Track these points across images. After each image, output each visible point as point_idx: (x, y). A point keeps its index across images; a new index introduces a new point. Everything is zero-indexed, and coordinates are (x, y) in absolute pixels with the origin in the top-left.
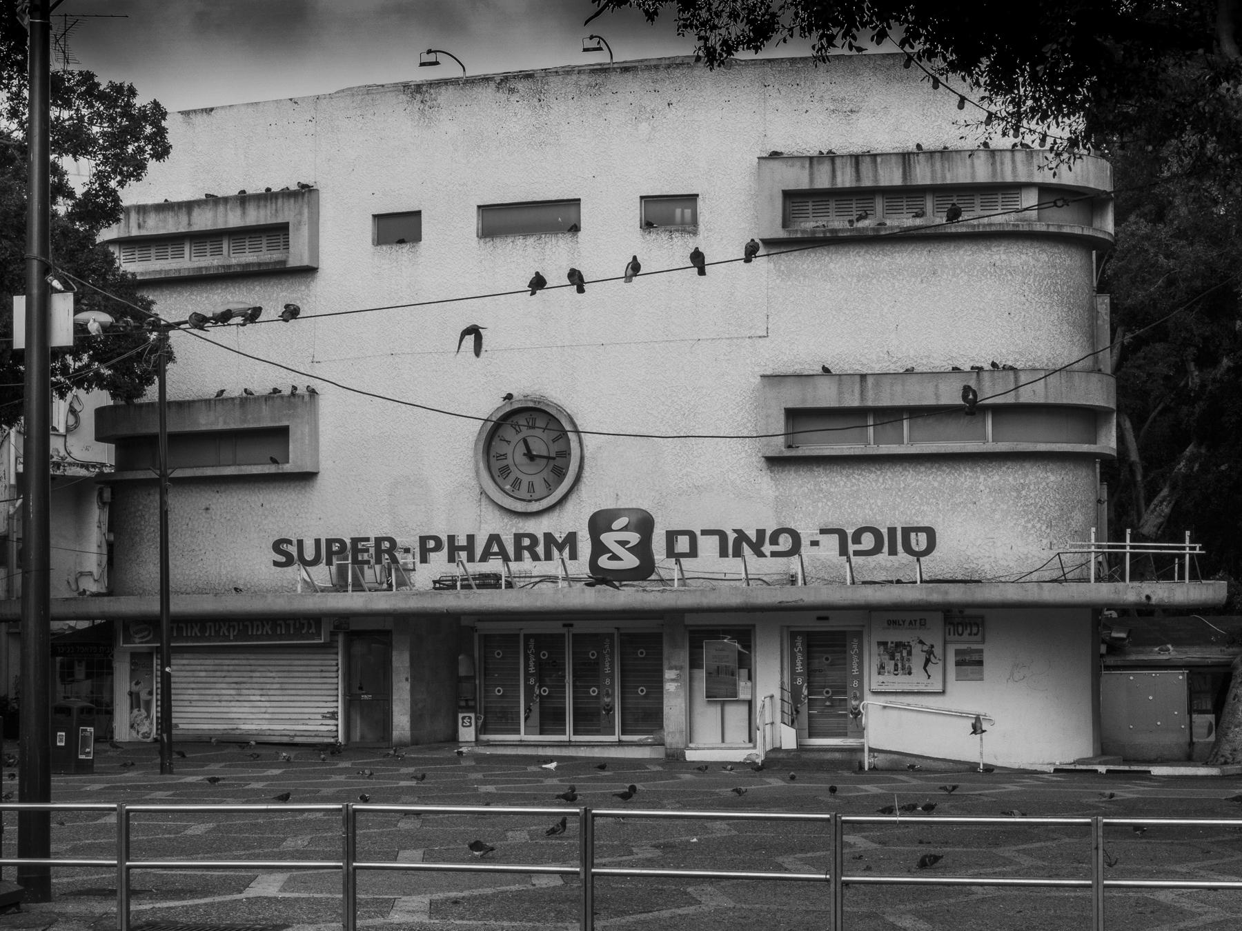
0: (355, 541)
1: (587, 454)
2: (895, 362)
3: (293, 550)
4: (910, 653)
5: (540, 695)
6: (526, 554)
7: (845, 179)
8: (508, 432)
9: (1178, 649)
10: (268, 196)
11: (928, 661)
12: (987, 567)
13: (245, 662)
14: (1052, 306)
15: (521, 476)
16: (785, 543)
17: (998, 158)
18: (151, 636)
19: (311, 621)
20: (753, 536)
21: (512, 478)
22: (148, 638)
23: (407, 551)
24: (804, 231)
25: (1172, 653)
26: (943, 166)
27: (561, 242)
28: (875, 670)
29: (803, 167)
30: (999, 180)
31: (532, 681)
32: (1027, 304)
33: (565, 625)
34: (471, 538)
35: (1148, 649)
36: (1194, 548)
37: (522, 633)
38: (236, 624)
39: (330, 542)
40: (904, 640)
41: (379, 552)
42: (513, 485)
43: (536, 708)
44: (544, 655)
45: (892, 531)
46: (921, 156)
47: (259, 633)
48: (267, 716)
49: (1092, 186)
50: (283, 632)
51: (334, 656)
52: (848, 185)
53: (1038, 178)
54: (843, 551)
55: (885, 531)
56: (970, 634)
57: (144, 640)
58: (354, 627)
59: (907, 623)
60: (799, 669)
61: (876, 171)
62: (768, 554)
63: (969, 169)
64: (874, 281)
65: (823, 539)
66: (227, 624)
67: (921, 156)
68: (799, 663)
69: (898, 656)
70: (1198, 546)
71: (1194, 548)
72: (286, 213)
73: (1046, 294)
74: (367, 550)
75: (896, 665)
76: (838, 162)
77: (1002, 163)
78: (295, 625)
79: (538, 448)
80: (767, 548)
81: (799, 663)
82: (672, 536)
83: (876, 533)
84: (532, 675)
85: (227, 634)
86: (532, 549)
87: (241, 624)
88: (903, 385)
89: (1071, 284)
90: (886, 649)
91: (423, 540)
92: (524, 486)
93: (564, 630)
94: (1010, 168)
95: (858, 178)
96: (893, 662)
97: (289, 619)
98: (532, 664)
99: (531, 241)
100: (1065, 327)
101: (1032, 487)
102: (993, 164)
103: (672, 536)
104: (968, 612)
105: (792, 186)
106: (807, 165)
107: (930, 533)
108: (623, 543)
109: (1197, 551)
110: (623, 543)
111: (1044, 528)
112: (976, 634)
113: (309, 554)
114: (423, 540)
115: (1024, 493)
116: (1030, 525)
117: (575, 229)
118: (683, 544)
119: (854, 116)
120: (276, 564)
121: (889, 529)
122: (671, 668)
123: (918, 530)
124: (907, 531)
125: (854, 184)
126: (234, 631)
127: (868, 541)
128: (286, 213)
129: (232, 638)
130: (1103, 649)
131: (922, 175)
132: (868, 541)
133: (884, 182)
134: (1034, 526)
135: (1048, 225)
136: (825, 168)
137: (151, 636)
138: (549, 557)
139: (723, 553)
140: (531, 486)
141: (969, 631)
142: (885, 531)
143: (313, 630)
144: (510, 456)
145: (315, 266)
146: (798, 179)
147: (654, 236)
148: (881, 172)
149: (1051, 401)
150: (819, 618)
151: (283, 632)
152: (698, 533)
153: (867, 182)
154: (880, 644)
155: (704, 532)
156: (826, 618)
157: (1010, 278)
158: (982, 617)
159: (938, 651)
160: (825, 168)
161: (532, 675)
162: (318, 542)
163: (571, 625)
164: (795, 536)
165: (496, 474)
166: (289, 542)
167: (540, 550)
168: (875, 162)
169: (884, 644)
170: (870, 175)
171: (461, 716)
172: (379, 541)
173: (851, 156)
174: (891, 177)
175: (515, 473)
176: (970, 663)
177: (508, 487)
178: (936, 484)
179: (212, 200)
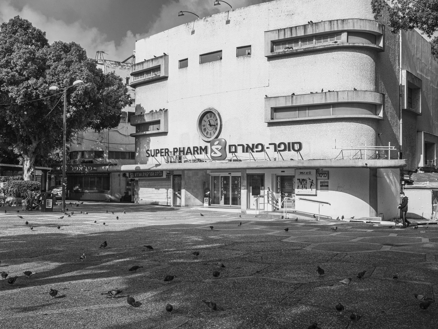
0: (161, 149)
1: (223, 123)
2: (304, 91)
4: (306, 183)
5: (224, 193)
6: (196, 153)
7: (288, 36)
8: (205, 118)
9: (431, 183)
10: (156, 58)
11: (311, 185)
12: (330, 155)
13: (145, 183)
14: (353, 70)
15: (209, 131)
16: (260, 148)
17: (332, 23)
20: (251, 146)
21: (206, 132)
23: (171, 152)
24: (276, 53)
25: (428, 184)
26: (316, 28)
27: (218, 63)
28: (296, 187)
29: (276, 33)
30: (333, 30)
31: (222, 189)
32: (344, 70)
33: (229, 174)
34: (184, 148)
35: (420, 183)
36: (392, 148)
37: (220, 176)
39: (156, 150)
40: (305, 178)
42: (207, 134)
43: (223, 197)
44: (225, 182)
45: (289, 143)
46: (309, 25)
48: (158, 198)
49: (368, 30)
51: (170, 182)
52: (289, 37)
53: (346, 28)
54: (275, 150)
55: (287, 144)
56: (324, 177)
58: (175, 174)
59: (305, 173)
60: (279, 187)
61: (297, 32)
62: (255, 151)
63: (323, 28)
64: (298, 67)
65: (270, 146)
67: (309, 25)
68: (279, 185)
69: (303, 183)
70: (393, 147)
71: (392, 148)
72: (161, 62)
73: (351, 66)
75: (302, 186)
76: (286, 30)
77: (334, 25)
79: (212, 123)
80: (255, 150)
81: (279, 185)
82: (230, 146)
83: (284, 144)
84: (222, 188)
86: (197, 151)
88: (304, 98)
89: (362, 62)
90: (299, 181)
91: (174, 149)
92: (209, 134)
93: (229, 175)
94: (336, 26)
95: (292, 34)
96: (301, 185)
98: (222, 185)
99: (211, 63)
100: (359, 77)
101: (345, 129)
102: (331, 25)
103: (230, 146)
104: (324, 169)
105: (273, 39)
106: (277, 32)
107: (300, 144)
108: (217, 149)
109: (393, 149)
110: (217, 149)
111: (349, 142)
112: (326, 177)
114: (174, 149)
115: (342, 131)
116: (344, 142)
117: (221, 58)
118: (233, 149)
119: (293, 16)
121: (288, 143)
122: (243, 186)
123: (297, 143)
124: (293, 144)
125: (290, 37)
127: (282, 147)
128: (161, 62)
130: (403, 183)
131: (310, 31)
132: (282, 147)
133: (299, 35)
134: (345, 142)
135: (349, 43)
136: (282, 32)
138: (201, 153)
139: (243, 152)
140: (211, 133)
141: (323, 176)
142: (287, 144)
144: (206, 125)
145: (167, 76)
146: (275, 37)
147: (240, 59)
148: (298, 32)
149: (350, 101)
150: (282, 172)
152: (237, 145)
153: (294, 36)
154: (298, 179)
155: (239, 145)
156: (284, 172)
157: (338, 62)
158: (328, 172)
159: (314, 182)
160: (282, 32)
161: (222, 188)
162: (154, 150)
163: (230, 174)
164: (262, 145)
165: (203, 130)
167: (199, 152)
168: (296, 29)
169: (299, 179)
170: (295, 33)
171: (205, 198)
172: (165, 149)
173: (289, 28)
174: (301, 33)
175: (207, 130)
176: (325, 186)
177: (205, 134)
178: (315, 129)
179: (146, 61)
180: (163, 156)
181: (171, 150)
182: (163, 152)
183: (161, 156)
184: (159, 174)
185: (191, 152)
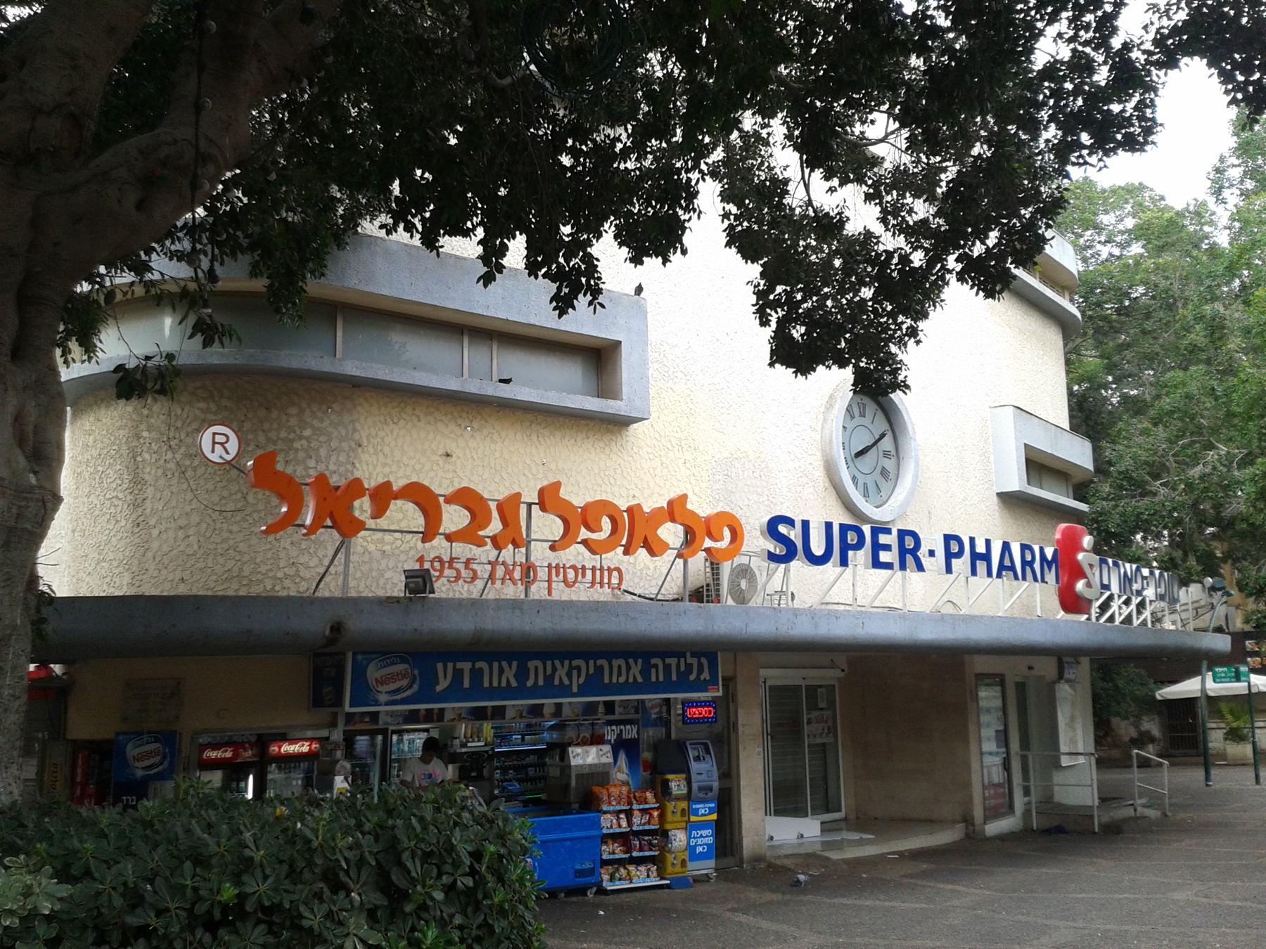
18: (416, 687)
22: (409, 693)
34: (988, 542)
38: (581, 663)
41: (903, 551)
47: (622, 680)
50: (661, 679)
57: (399, 697)
66: (567, 663)
74: (887, 548)
78: (678, 665)
85: (566, 682)
87: (591, 662)
97: (671, 655)
113: (818, 549)
126: (579, 676)
129: (575, 689)
137: (416, 687)
143: (706, 675)
151: (661, 679)
172: (902, 534)
180: (888, 566)
181: (932, 540)
182: (887, 548)
184: (684, 675)
185: (1012, 568)
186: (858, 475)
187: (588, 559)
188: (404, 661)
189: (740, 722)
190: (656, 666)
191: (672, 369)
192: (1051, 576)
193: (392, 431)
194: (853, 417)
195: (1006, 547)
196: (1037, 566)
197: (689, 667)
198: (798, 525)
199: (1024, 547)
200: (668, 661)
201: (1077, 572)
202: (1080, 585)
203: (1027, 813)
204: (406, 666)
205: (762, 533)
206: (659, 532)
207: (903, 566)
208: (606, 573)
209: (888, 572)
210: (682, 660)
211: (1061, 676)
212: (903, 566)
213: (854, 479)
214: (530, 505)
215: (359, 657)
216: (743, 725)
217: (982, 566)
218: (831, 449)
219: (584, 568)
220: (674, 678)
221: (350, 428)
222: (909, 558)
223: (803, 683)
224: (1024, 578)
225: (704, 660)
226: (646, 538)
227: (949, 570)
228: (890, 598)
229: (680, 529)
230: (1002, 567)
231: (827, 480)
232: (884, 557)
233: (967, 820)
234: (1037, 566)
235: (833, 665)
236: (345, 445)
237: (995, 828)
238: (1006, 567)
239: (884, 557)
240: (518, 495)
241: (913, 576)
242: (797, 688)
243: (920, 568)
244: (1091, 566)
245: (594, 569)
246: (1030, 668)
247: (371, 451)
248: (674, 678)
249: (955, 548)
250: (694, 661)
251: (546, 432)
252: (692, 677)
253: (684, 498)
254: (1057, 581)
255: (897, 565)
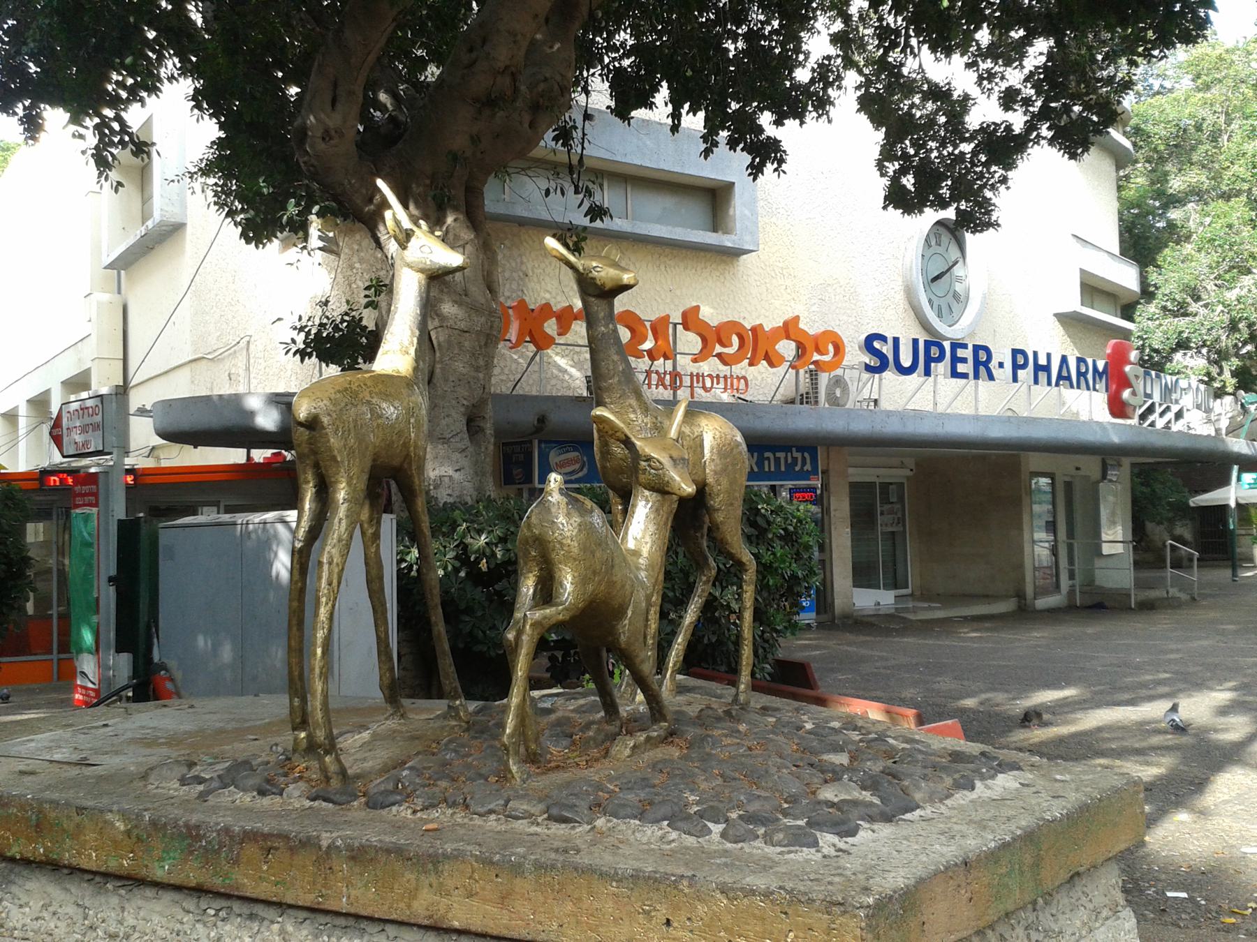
3: (887, 349)
18: (585, 470)
19: (806, 455)
22: (580, 474)
34: (1049, 356)
41: (977, 363)
50: (772, 469)
57: (573, 478)
74: (964, 360)
91: (1015, 352)
113: (906, 362)
114: (1015, 352)
120: (868, 368)
137: (585, 470)
143: (808, 467)
151: (772, 469)
162: (915, 342)
166: (883, 338)
172: (977, 348)
181: (1001, 354)
182: (964, 360)
183: (955, 374)
185: (1069, 378)
186: (933, 298)
187: (724, 370)
188: (575, 449)
189: (832, 508)
190: (768, 459)
191: (775, 206)
192: (1101, 385)
193: (550, 264)
194: (930, 246)
195: (1064, 359)
196: (1090, 376)
197: (795, 460)
198: (890, 342)
199: (1080, 360)
200: (778, 455)
201: (1124, 382)
202: (1126, 394)
203: (1071, 592)
204: (577, 454)
205: (860, 348)
206: (777, 347)
207: (976, 376)
208: (735, 381)
209: (963, 381)
210: (789, 454)
211: (1104, 477)
212: (976, 376)
213: (930, 301)
214: (675, 325)
215: (543, 446)
216: (835, 510)
217: (1042, 376)
218: (911, 275)
219: (718, 376)
220: (783, 469)
221: (518, 260)
222: (982, 368)
223: (877, 481)
224: (1079, 387)
225: (806, 455)
226: (767, 352)
227: (1015, 379)
228: (963, 407)
229: (793, 345)
230: (1060, 377)
231: (906, 303)
232: (961, 368)
233: (1020, 595)
234: (1090, 376)
235: (902, 466)
236: (515, 275)
237: (1042, 603)
238: (1063, 378)
239: (961, 368)
240: (668, 316)
241: (983, 384)
242: (871, 485)
243: (991, 377)
244: (1137, 377)
245: (725, 377)
246: (1078, 469)
247: (535, 279)
248: (783, 469)
249: (1021, 361)
250: (798, 455)
251: (672, 263)
252: (797, 468)
253: (797, 318)
254: (1107, 391)
255: (971, 375)
